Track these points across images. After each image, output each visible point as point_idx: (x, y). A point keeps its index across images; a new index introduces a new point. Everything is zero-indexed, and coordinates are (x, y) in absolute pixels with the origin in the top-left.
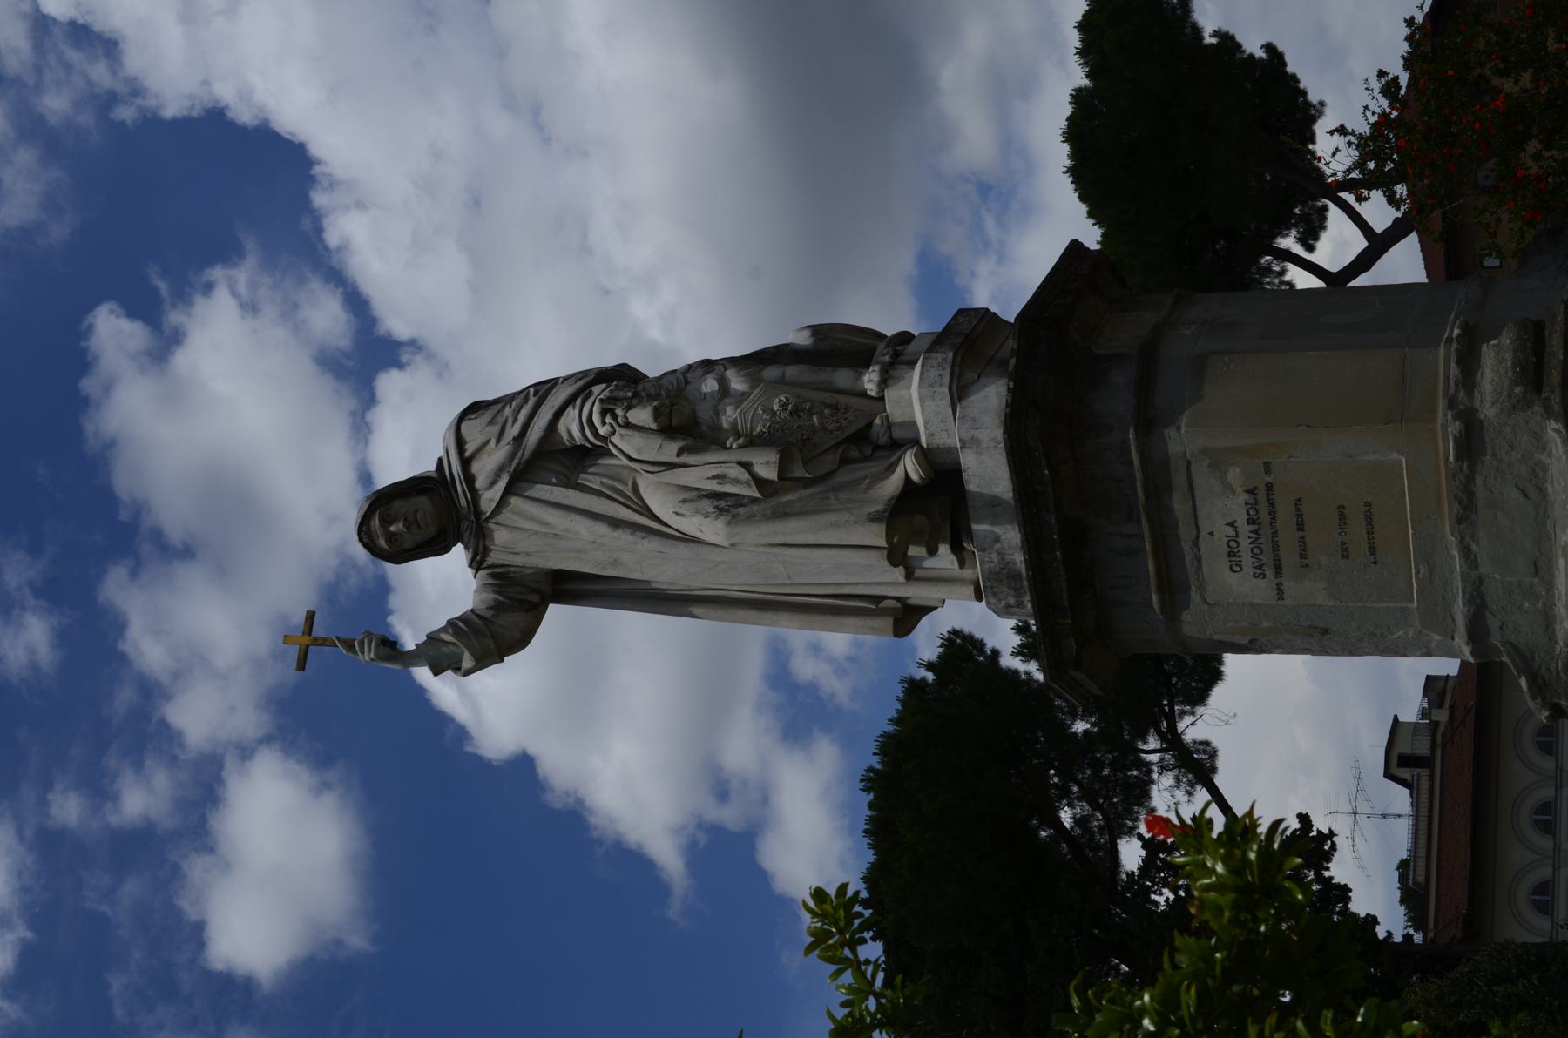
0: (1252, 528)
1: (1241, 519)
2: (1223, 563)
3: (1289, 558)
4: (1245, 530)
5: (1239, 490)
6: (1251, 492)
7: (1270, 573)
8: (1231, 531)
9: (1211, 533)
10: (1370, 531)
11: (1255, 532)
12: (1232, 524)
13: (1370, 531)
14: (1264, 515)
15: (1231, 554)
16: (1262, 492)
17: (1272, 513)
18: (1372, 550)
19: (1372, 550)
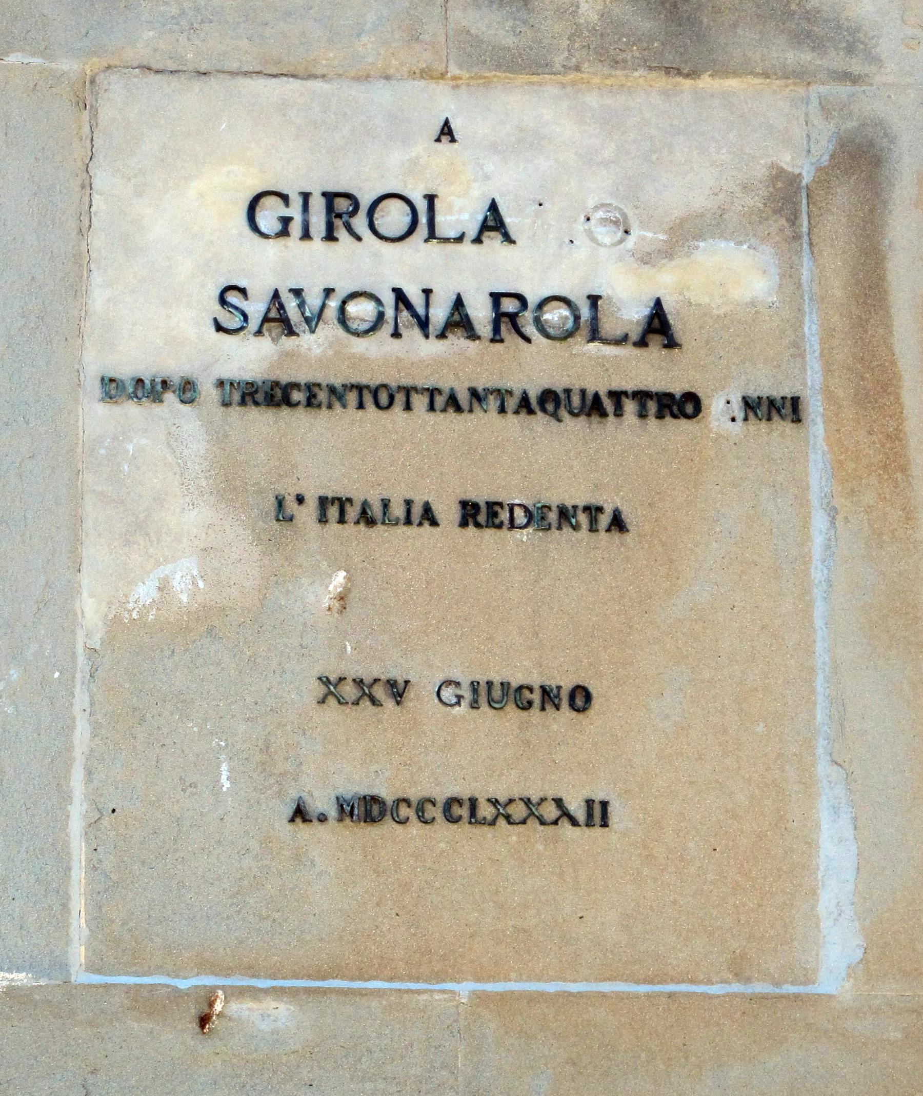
0: (480, 312)
1: (523, 268)
2: (305, 170)
3: (324, 451)
4: (470, 275)
5: (667, 283)
6: (658, 327)
7: (253, 357)
8: (460, 213)
9: (446, 132)
10: (460, 810)
11: (459, 321)
12: (493, 223)
13: (460, 810)
14: (534, 365)
15: (340, 212)
16: (649, 370)
17: (551, 402)
18: (367, 810)
19: (367, 810)
